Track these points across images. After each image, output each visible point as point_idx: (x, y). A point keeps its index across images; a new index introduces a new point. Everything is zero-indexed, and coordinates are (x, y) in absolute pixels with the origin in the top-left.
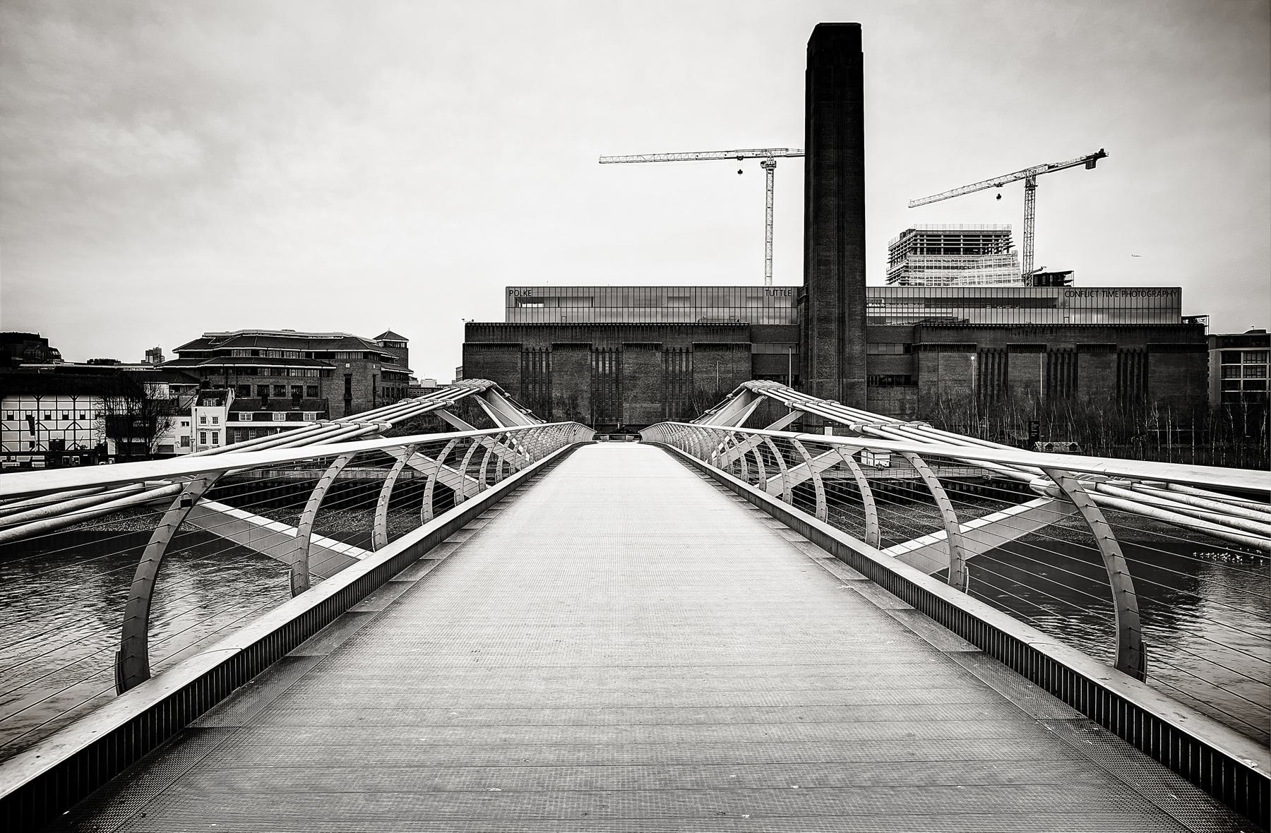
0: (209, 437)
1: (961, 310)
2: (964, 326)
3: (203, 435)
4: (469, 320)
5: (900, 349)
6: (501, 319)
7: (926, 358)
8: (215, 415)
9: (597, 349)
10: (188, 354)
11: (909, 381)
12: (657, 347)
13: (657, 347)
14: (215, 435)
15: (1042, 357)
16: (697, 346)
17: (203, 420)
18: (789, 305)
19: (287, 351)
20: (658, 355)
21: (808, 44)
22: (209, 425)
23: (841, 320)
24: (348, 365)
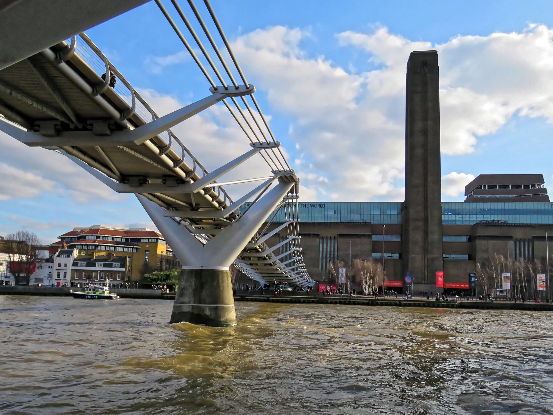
2: (505, 225)
3: (59, 273)
5: (464, 239)
7: (480, 244)
8: (66, 263)
9: (283, 237)
10: (64, 238)
12: (317, 235)
13: (317, 235)
14: (65, 273)
16: (341, 235)
17: (60, 265)
18: (396, 213)
19: (115, 237)
20: (318, 240)
22: (63, 267)
23: (426, 220)
24: (147, 246)
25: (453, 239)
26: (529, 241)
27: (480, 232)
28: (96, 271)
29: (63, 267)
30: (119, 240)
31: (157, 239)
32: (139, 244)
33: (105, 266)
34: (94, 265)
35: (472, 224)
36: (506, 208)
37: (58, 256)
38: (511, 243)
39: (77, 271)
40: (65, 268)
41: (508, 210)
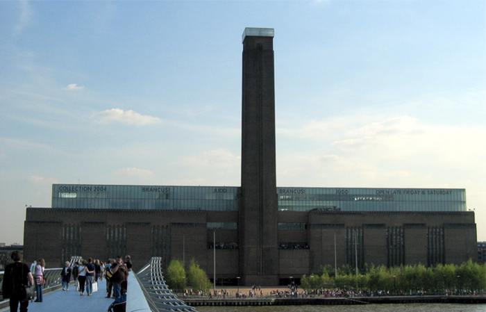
1: (338, 202)
2: (337, 212)
4: (28, 206)
7: (315, 232)
11: (305, 245)
13: (148, 224)
15: (383, 233)
16: (174, 224)
18: (232, 198)
21: (243, 43)
35: (308, 209)
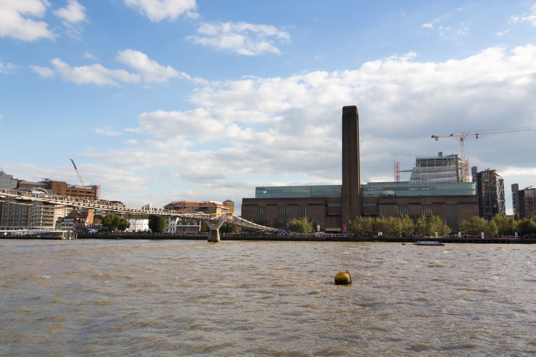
0: (172, 229)
3: (171, 228)
4: (244, 197)
5: (375, 205)
6: (254, 196)
12: (297, 205)
13: (297, 205)
14: (174, 228)
17: (171, 225)
20: (297, 207)
22: (173, 225)
23: (350, 196)
25: (369, 205)
26: (406, 205)
27: (381, 202)
28: (187, 227)
29: (173, 225)
30: (196, 208)
31: (216, 207)
32: (207, 210)
33: (191, 224)
34: (186, 224)
36: (399, 186)
37: (171, 220)
38: (396, 207)
39: (179, 227)
40: (173, 226)
41: (400, 188)
